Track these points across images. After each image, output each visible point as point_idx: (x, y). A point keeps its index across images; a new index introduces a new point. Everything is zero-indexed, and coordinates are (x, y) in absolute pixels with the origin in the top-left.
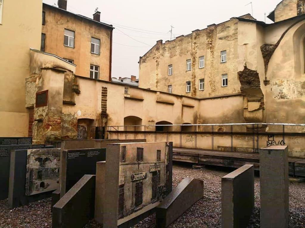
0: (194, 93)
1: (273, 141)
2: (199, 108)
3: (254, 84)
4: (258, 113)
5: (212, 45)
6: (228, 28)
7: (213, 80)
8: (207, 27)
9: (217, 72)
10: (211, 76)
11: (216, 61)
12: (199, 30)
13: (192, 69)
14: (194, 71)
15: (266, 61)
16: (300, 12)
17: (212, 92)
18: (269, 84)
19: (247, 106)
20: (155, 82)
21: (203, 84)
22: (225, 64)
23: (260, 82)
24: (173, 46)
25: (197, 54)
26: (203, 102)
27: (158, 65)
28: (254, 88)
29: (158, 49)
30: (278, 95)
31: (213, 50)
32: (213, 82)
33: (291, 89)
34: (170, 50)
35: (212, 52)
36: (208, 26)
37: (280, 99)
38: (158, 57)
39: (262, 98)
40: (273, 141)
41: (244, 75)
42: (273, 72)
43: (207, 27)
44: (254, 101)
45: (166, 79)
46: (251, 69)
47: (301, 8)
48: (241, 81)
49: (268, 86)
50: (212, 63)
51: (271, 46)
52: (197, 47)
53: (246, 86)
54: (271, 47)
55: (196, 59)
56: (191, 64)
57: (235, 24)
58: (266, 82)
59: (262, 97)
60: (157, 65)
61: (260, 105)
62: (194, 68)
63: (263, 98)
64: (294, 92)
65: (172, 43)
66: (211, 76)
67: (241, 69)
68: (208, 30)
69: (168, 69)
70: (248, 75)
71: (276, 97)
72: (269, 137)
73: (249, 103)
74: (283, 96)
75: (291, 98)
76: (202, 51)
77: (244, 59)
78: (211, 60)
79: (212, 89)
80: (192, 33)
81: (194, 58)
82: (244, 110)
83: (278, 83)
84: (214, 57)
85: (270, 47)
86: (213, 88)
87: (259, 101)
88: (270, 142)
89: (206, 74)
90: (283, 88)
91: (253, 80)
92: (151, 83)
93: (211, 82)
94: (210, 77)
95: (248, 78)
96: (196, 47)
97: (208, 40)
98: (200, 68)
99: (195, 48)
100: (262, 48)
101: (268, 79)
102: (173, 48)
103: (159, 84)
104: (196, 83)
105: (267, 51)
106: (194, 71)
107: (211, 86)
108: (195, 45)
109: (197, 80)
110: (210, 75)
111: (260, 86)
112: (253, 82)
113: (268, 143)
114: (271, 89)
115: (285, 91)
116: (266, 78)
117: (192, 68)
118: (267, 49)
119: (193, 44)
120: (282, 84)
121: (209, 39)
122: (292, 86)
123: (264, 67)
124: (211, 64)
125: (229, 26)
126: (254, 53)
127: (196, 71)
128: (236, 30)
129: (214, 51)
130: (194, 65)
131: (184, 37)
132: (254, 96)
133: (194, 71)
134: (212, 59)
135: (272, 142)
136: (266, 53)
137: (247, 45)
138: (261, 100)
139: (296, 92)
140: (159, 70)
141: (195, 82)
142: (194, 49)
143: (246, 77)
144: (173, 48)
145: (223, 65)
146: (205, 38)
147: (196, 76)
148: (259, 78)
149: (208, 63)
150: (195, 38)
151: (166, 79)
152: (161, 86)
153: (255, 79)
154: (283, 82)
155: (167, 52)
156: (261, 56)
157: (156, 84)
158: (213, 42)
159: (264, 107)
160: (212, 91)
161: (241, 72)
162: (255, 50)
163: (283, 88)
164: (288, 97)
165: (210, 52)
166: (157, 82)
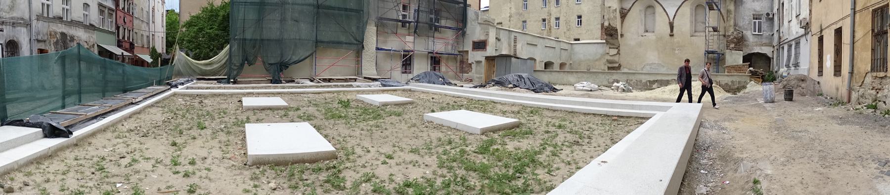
0: (549, 31)
9: (572, 12)
22: (579, 5)
32: (568, 22)
44: (613, 48)
58: (622, 35)
70: (611, 29)
73: (611, 49)
86: (568, 27)
87: (617, 49)
92: (503, 17)
103: (512, 18)
110: (565, 14)
127: (552, 9)
132: (613, 45)
138: (618, 48)
140: (512, 3)
145: (577, 5)
151: (521, 15)
152: (515, 20)
166: (510, 17)
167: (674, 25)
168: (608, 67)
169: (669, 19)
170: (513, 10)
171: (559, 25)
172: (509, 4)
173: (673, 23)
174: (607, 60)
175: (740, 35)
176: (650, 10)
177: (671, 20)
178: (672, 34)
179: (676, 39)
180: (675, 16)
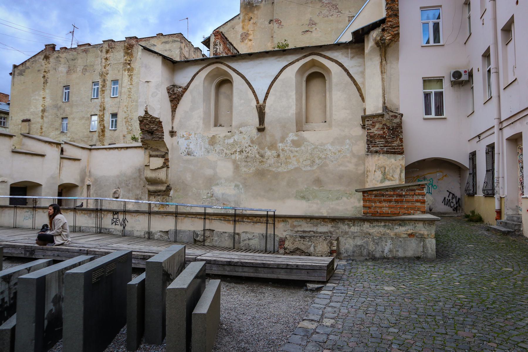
1: (117, 219)
2: (88, 162)
3: (157, 135)
4: (161, 172)
5: (130, 66)
6: (154, 46)
7: (130, 116)
8: (125, 39)
10: (127, 110)
11: (135, 90)
12: (114, 41)
13: (99, 97)
14: (104, 100)
15: (174, 106)
16: (216, 52)
17: (128, 134)
18: (175, 136)
19: (149, 162)
20: (41, 110)
21: (116, 121)
23: (163, 133)
24: (71, 57)
25: (108, 75)
26: (94, 153)
27: (46, 82)
28: (157, 139)
29: (47, 58)
30: (185, 151)
31: (132, 74)
32: (129, 120)
33: (198, 145)
34: (68, 63)
35: (130, 77)
36: (126, 38)
37: (186, 155)
38: (46, 70)
39: (167, 153)
40: (117, 219)
41: (145, 121)
42: (180, 121)
43: (125, 39)
44: (157, 156)
45: (59, 108)
46: (153, 115)
47: (218, 47)
48: (141, 129)
49: (174, 138)
50: (129, 92)
51: (180, 89)
52: (109, 65)
53: (149, 137)
54: (180, 90)
55: (106, 82)
56: (100, 90)
57: (162, 43)
58: (172, 133)
59: (167, 151)
60: (44, 83)
61: (164, 163)
62: (103, 95)
63: (167, 153)
64: (201, 148)
65: (71, 52)
66: (127, 110)
67: (142, 114)
68: (126, 44)
69: (63, 92)
71: (183, 153)
72: (114, 214)
73: (152, 159)
74: (190, 152)
75: (198, 155)
76: (116, 72)
77: (144, 101)
78: (128, 88)
79: (127, 129)
80: (102, 42)
81: (104, 81)
82: (146, 168)
83: (185, 136)
84: (133, 83)
85: (178, 89)
86: (130, 128)
87: (163, 156)
88: (115, 220)
89: (120, 108)
90: (191, 142)
91: (156, 130)
93: (127, 119)
94: (125, 112)
95: (150, 126)
96: (108, 65)
97: (126, 57)
98: (112, 97)
99: (105, 66)
100: (168, 89)
101: (175, 130)
102: (72, 60)
103: (46, 114)
104: (105, 119)
105: (175, 94)
106: (104, 100)
107: (127, 124)
108: (106, 62)
109: (107, 114)
110: (125, 109)
111: (163, 138)
112: (155, 131)
113: (113, 222)
114: (178, 142)
115: (192, 146)
116: (173, 128)
117: (101, 95)
118: (175, 92)
119: (104, 61)
120: (189, 138)
121: (127, 57)
122: (200, 140)
123: (171, 114)
124: (128, 93)
125: (155, 44)
126: (157, 95)
127: (106, 100)
128: (163, 51)
129: (132, 75)
130: (103, 91)
131: (91, 47)
132: (158, 150)
133: (103, 100)
134: (131, 86)
135: (116, 220)
136: (174, 97)
137: (150, 83)
138: (164, 156)
139: (203, 148)
140: (47, 91)
141: (104, 117)
142: (105, 68)
143: (147, 124)
144: (72, 60)
146: (122, 53)
147: (106, 108)
148: (163, 128)
149: (124, 92)
150: (107, 52)
151: (59, 108)
152: (50, 117)
153: (158, 128)
154: (190, 135)
155: (62, 66)
156: (168, 99)
157: (41, 114)
158: (132, 62)
159: (168, 165)
160: (127, 132)
161: (142, 117)
162: (159, 91)
163: (191, 142)
164: (195, 154)
165: (128, 76)
166: (43, 111)
167: (267, 110)
168: (149, 191)
169: (257, 101)
170: (48, 102)
171: (116, 125)
172: (42, 93)
173: (264, 107)
174: (146, 178)
175: (397, 120)
176: (224, 89)
177: (261, 102)
178: (262, 127)
179: (268, 138)
180: (268, 93)
